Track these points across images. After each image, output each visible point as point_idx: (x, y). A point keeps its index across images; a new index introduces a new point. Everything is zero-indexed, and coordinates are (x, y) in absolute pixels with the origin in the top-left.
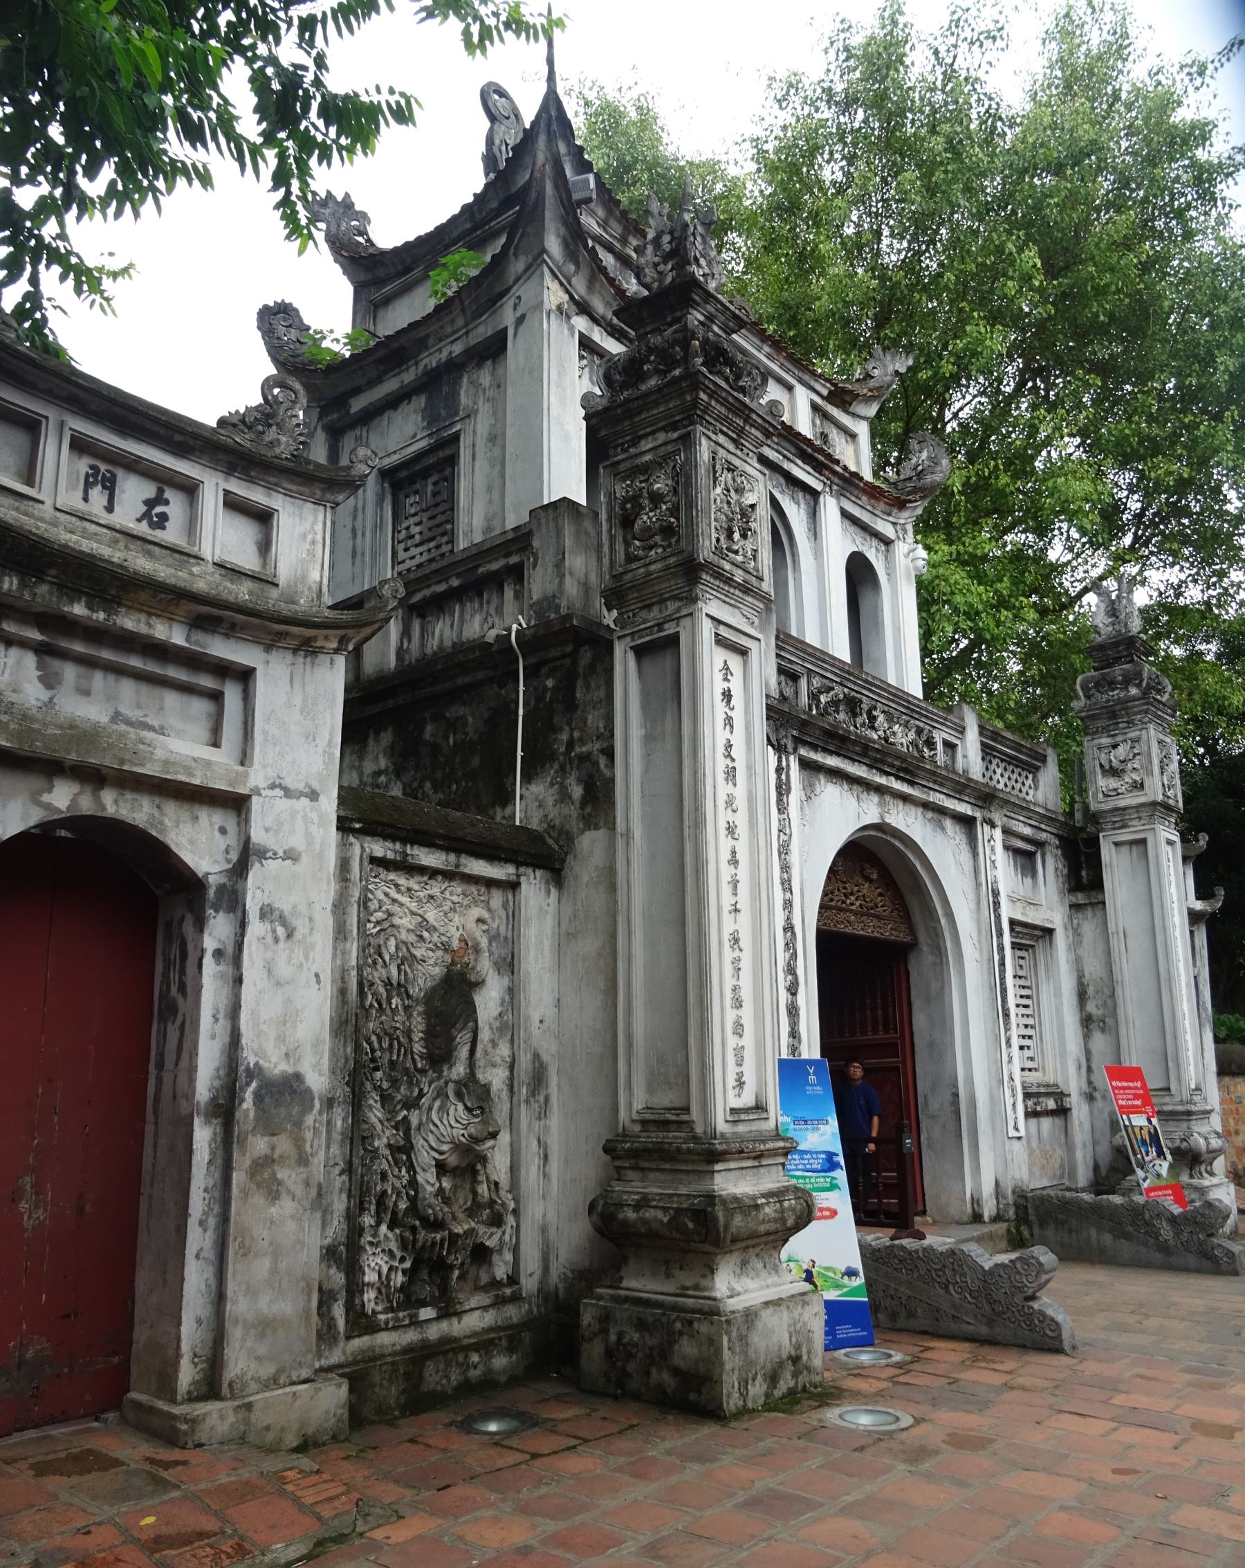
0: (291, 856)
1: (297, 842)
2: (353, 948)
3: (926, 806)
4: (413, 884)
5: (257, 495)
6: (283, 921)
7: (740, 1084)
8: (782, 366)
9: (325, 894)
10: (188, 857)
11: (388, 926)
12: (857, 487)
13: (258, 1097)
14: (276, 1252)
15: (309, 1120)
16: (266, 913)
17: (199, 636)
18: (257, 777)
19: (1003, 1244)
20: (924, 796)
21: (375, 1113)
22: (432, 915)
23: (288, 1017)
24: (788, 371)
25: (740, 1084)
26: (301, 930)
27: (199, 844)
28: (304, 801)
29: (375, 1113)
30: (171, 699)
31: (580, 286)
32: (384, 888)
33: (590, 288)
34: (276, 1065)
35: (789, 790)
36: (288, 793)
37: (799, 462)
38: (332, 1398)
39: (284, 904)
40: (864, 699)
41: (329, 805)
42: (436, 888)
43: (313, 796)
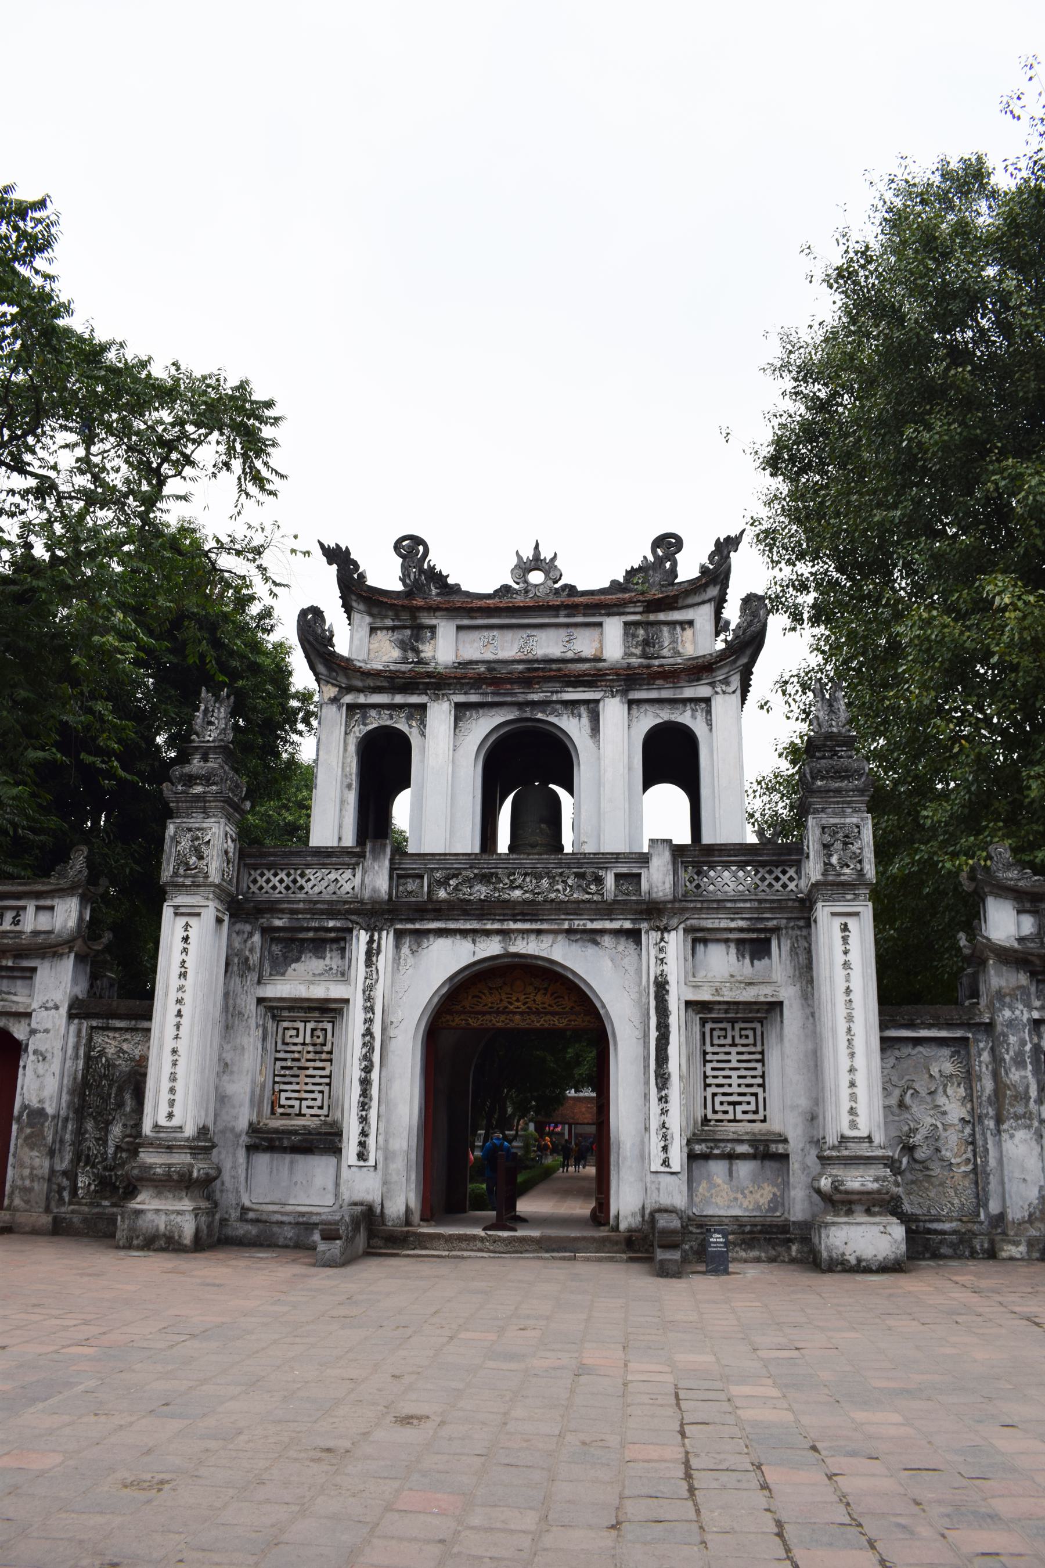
0: (47, 1031)
1: (49, 1026)
2: (81, 1063)
3: (569, 932)
4: (117, 1035)
5: (48, 902)
6: (42, 1054)
7: (170, 1116)
8: (584, 615)
9: (58, 1044)
10: (16, 1035)
11: (102, 1053)
12: (644, 679)
13: (28, 1115)
14: (32, 1168)
15: (47, 1124)
16: (35, 1052)
17: (17, 961)
18: (35, 1005)
19: (623, 1247)
20: (556, 927)
21: (90, 1125)
22: (125, 1046)
23: (41, 1088)
24: (594, 615)
25: (170, 1116)
26: (49, 1056)
27: (19, 1031)
28: (53, 1011)
29: (90, 1125)
30: (19, 982)
31: (343, 681)
32: (99, 1039)
33: (348, 678)
34: (35, 1104)
35: (379, 952)
36: (47, 1009)
37: (570, 689)
38: (46, 1220)
39: (42, 1048)
40: (500, 871)
41: (64, 1010)
42: (128, 1036)
43: (57, 1007)
